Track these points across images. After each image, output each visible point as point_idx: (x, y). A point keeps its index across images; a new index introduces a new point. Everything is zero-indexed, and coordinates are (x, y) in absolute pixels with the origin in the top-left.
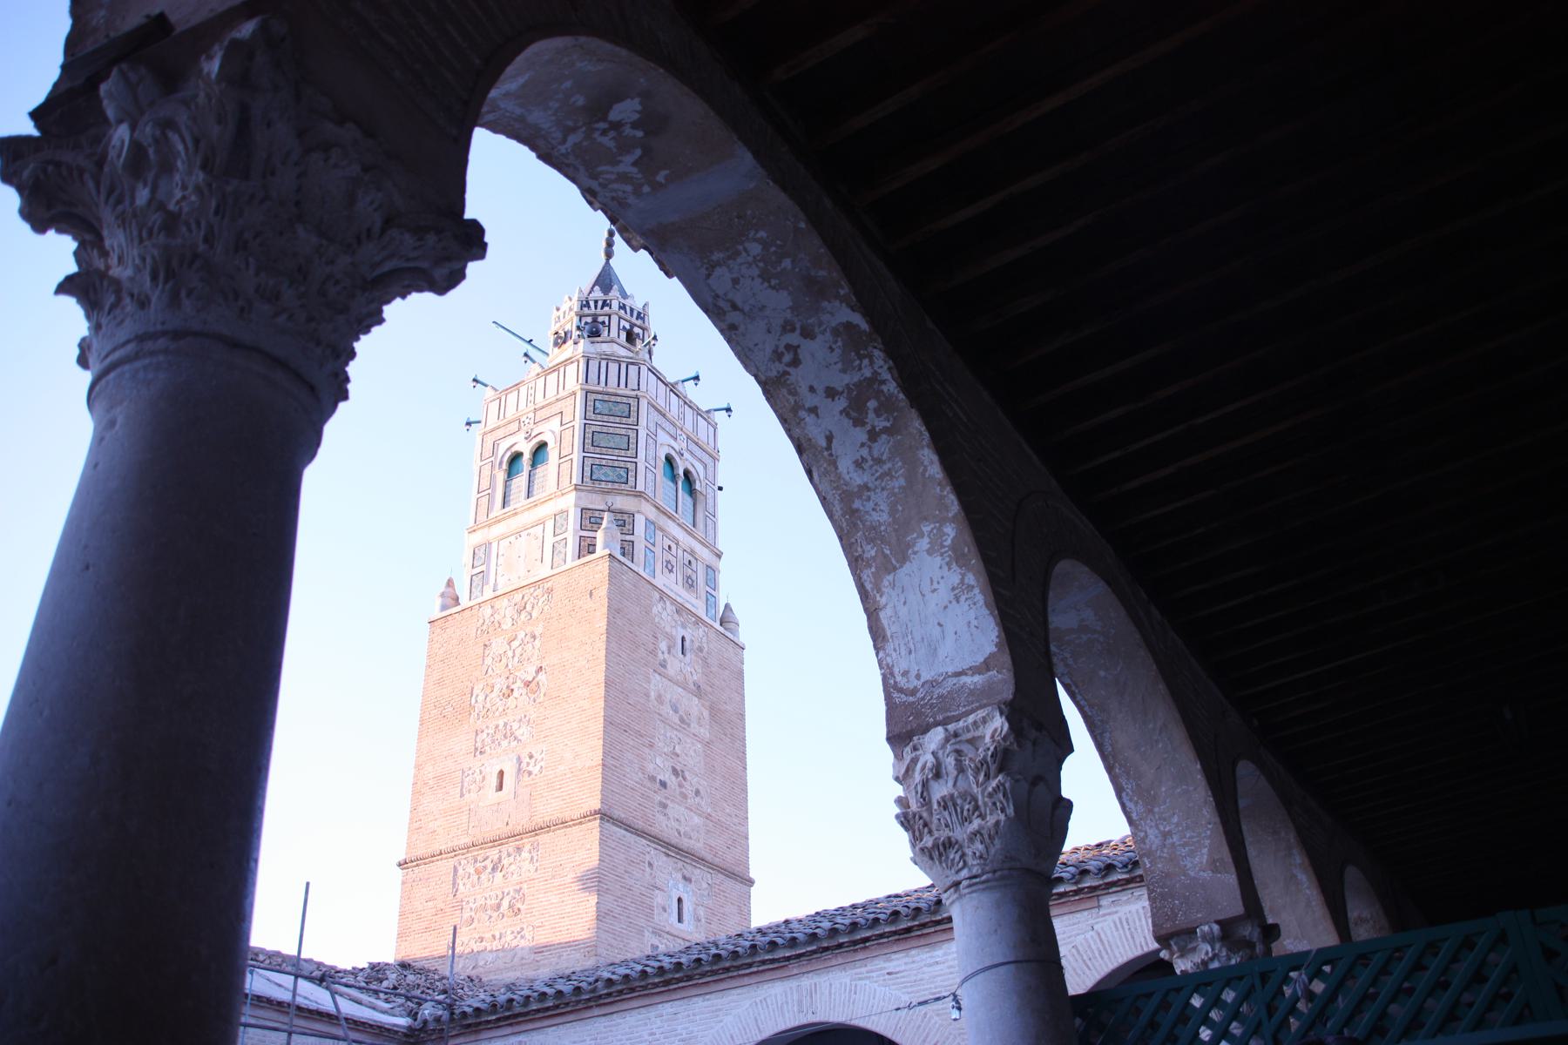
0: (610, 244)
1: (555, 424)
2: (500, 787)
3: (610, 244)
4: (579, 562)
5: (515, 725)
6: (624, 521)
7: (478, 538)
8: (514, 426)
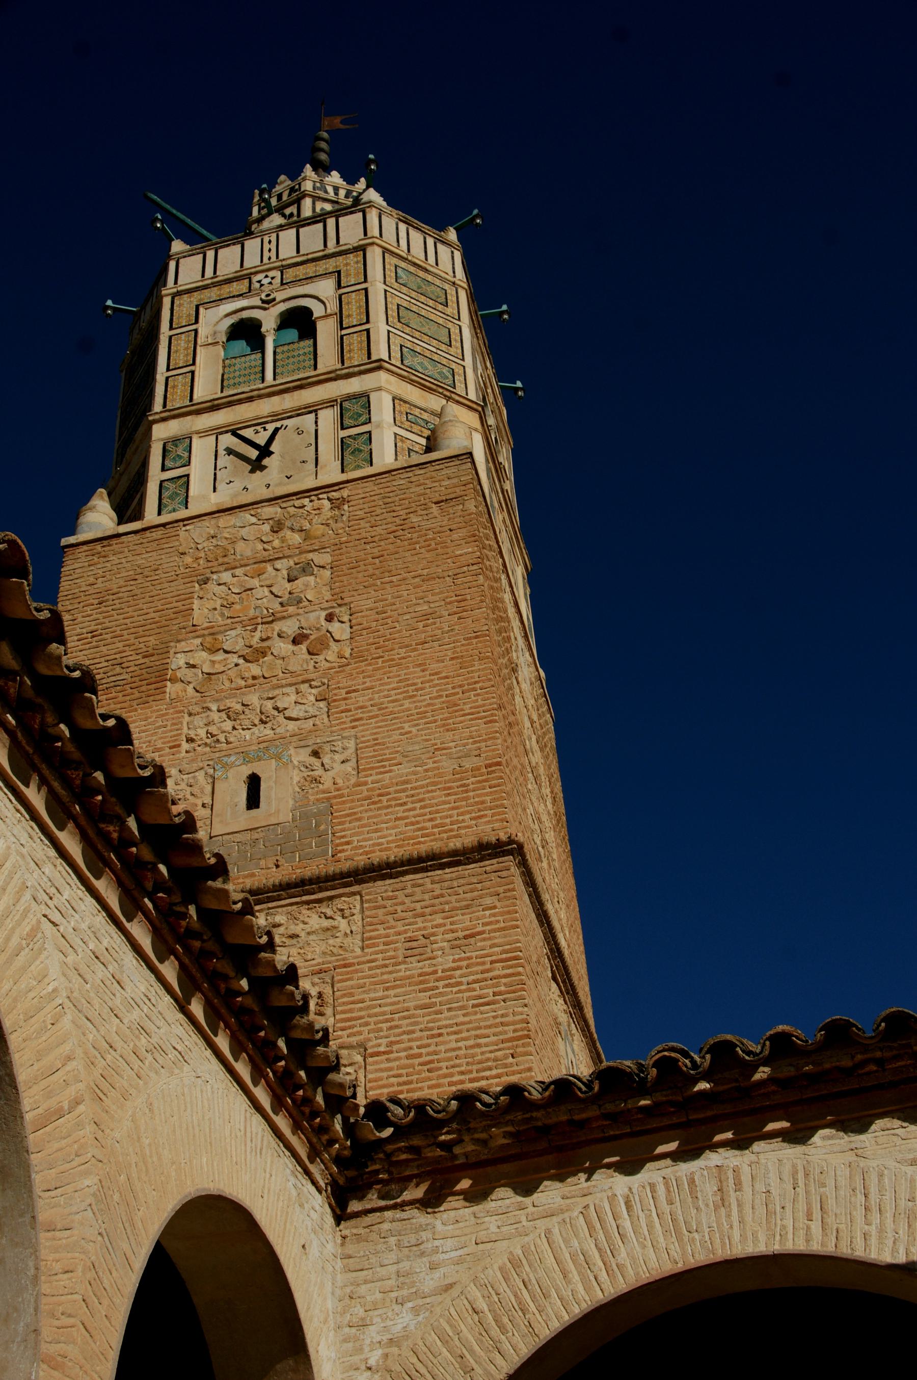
1: (326, 288)
2: (253, 801)
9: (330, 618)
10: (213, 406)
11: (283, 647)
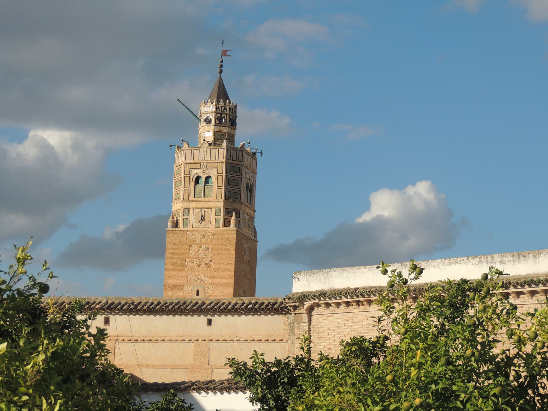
0: (222, 66)
1: (215, 171)
3: (222, 66)
4: (225, 228)
5: (203, 277)
6: (237, 216)
7: (185, 205)
8: (198, 166)
9: (211, 261)
10: (193, 201)
11: (203, 265)
